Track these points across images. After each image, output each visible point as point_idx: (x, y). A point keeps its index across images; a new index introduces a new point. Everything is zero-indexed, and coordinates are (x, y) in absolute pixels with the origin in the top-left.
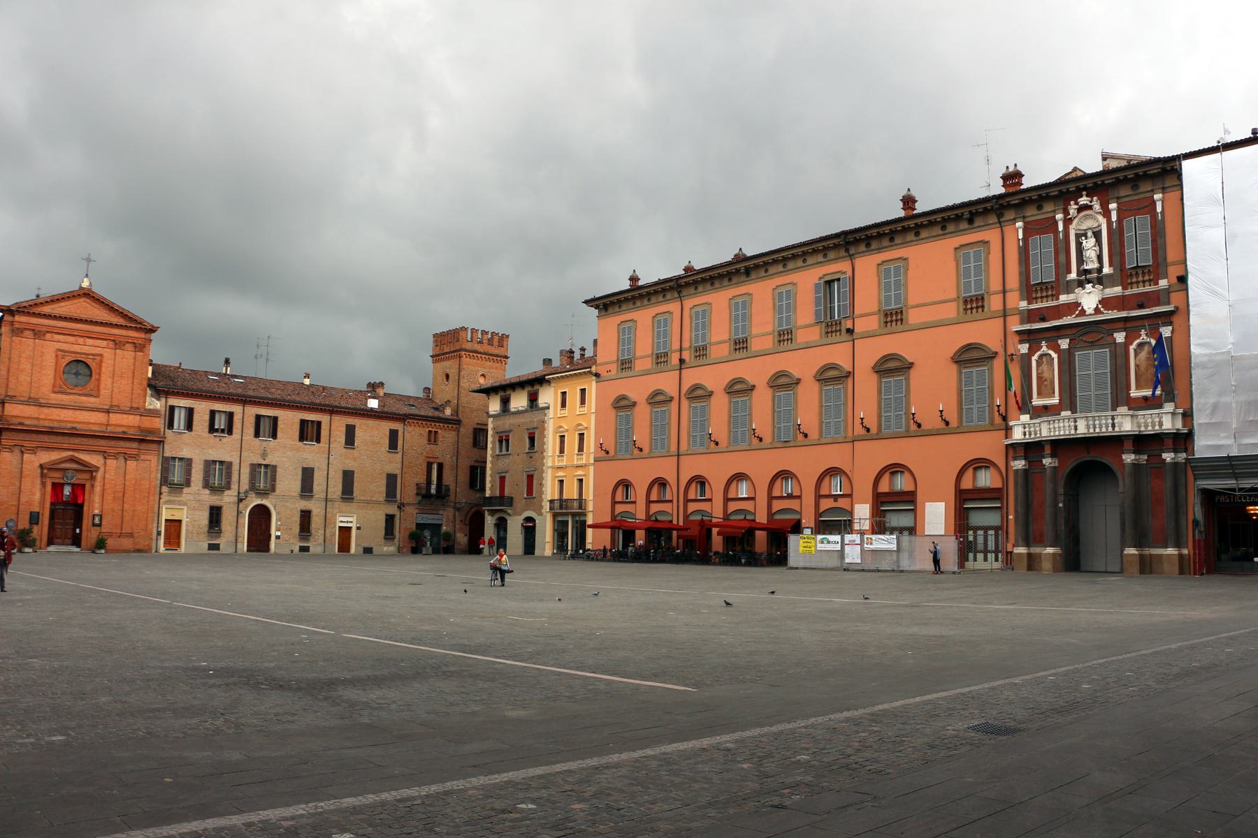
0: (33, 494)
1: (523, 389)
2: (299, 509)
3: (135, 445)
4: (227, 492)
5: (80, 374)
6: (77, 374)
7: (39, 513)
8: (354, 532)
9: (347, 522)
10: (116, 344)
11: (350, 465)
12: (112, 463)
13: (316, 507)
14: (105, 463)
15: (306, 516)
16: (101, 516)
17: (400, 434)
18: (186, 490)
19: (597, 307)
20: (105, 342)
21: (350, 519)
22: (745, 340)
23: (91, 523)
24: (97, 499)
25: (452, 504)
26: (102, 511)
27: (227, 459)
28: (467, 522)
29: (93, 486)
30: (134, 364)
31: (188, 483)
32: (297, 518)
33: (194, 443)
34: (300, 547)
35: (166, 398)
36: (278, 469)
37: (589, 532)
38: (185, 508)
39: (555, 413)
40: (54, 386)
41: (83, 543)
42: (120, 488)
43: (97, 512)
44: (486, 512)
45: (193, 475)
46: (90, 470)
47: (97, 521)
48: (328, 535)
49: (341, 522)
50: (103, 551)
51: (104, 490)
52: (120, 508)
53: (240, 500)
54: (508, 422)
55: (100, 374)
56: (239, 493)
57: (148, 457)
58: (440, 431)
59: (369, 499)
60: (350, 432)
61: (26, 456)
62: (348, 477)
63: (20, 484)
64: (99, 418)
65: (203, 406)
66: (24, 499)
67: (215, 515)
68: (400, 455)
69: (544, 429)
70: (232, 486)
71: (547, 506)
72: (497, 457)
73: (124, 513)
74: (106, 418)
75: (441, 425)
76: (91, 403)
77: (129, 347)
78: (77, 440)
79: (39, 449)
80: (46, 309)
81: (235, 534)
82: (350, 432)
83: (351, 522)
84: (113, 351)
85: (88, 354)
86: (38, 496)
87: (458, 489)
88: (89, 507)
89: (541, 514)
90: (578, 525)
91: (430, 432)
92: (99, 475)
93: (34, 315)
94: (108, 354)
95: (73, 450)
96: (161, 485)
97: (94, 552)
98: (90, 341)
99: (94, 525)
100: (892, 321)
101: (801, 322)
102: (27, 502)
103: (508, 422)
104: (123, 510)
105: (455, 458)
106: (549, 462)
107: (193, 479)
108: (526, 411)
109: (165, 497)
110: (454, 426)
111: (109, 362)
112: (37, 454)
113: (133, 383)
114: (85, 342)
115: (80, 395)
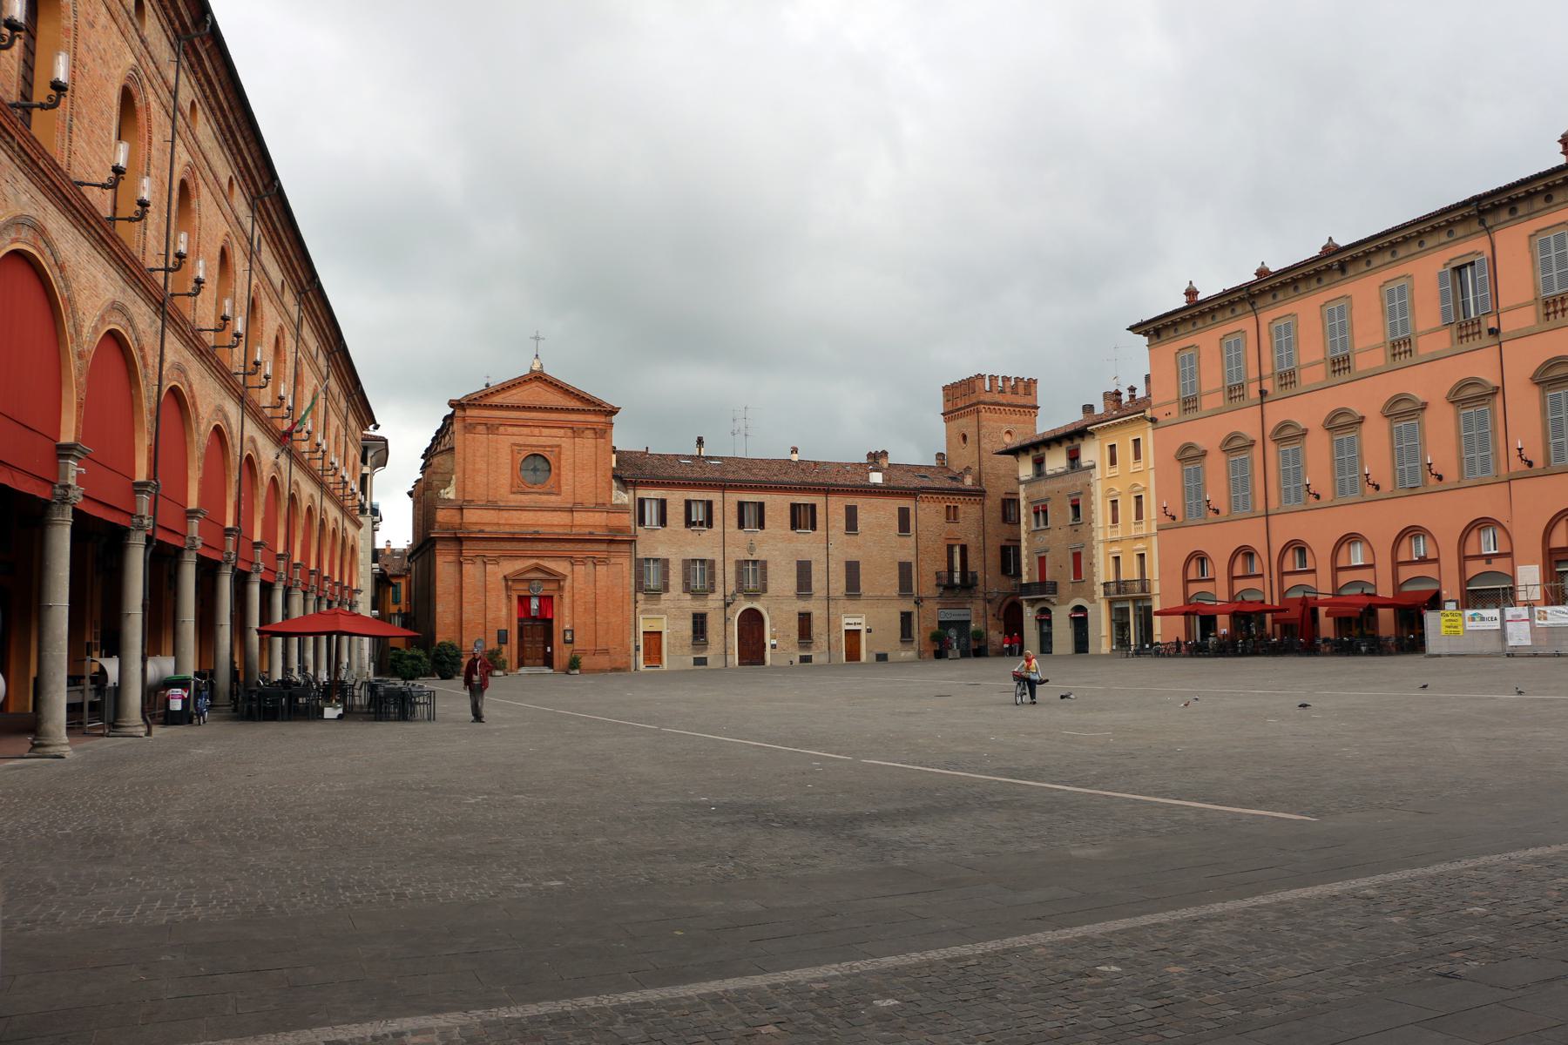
0: (500, 610)
1: (1061, 446)
2: (796, 611)
3: (604, 547)
4: (711, 596)
5: (538, 470)
6: (535, 470)
7: (506, 631)
8: (863, 635)
9: (855, 624)
10: (574, 432)
11: (854, 555)
12: (579, 569)
13: (816, 608)
15: (805, 619)
16: (573, 631)
17: (912, 512)
18: (664, 596)
19: (1146, 334)
20: (562, 431)
21: (858, 620)
22: (1346, 358)
23: (562, 640)
24: (567, 612)
25: (981, 595)
26: (573, 626)
27: (708, 557)
28: (1001, 617)
29: (561, 597)
30: (596, 454)
31: (666, 588)
32: (795, 623)
33: (670, 540)
34: (801, 657)
36: (768, 565)
37: (1157, 620)
38: (665, 617)
39: (1103, 471)
40: (512, 486)
41: (556, 663)
42: (591, 598)
43: (567, 626)
44: (1024, 602)
45: (671, 578)
46: (557, 579)
47: (568, 637)
48: (832, 641)
49: (848, 624)
50: (577, 672)
51: (573, 601)
52: (593, 621)
53: (727, 605)
54: (1044, 489)
55: (559, 468)
56: (725, 596)
57: (620, 560)
58: (960, 506)
59: (879, 594)
60: (851, 514)
61: (488, 567)
62: (852, 569)
66: (490, 616)
67: (699, 622)
68: (913, 538)
69: (1090, 494)
70: (717, 589)
71: (1100, 591)
72: (1033, 533)
74: (571, 518)
75: (962, 498)
77: (589, 434)
78: (540, 546)
79: (502, 558)
80: (497, 400)
81: (723, 646)
82: (851, 514)
83: (860, 624)
84: (572, 440)
85: (545, 447)
86: (504, 612)
87: (987, 576)
88: (559, 621)
89: (1093, 601)
90: (1142, 612)
91: (947, 507)
92: (567, 584)
93: (486, 407)
94: (566, 443)
96: (636, 592)
97: (567, 673)
98: (546, 431)
99: (566, 642)
100: (1555, 312)
101: (1421, 327)
102: (493, 619)
103: (1044, 489)
104: (596, 623)
105: (981, 538)
106: (1099, 535)
107: (671, 583)
108: (1066, 473)
109: (641, 606)
110: (978, 499)
111: (568, 453)
112: (501, 564)
114: (540, 432)
115: (540, 494)
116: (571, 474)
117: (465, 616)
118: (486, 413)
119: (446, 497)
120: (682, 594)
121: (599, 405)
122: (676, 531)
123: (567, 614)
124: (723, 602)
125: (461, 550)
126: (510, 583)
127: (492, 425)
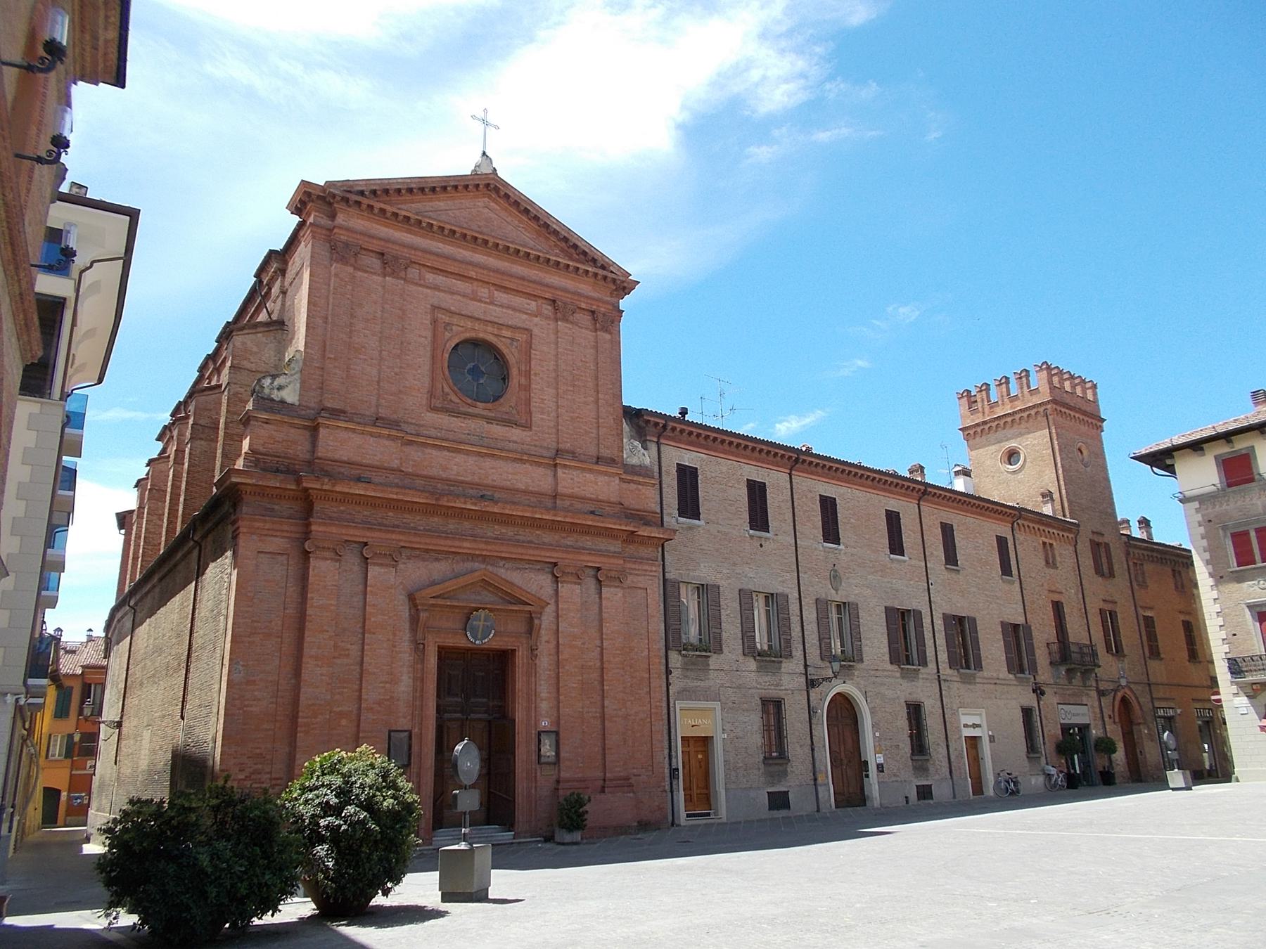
1: (1204, 455)
3: (615, 546)
6: (475, 372)
8: (986, 741)
10: (556, 309)
14: (557, 591)
16: (557, 733)
21: (977, 720)
24: (544, 690)
26: (558, 724)
27: (777, 588)
29: (533, 651)
33: (717, 550)
35: (658, 444)
38: (717, 705)
40: (431, 394)
41: (520, 815)
43: (545, 724)
47: (547, 749)
49: (966, 726)
50: (577, 836)
53: (811, 684)
55: (528, 374)
56: (806, 666)
61: (373, 571)
63: (363, 650)
64: (534, 478)
65: (724, 469)
66: (372, 694)
74: (550, 479)
76: (515, 442)
77: (585, 319)
79: (408, 552)
80: (409, 208)
81: (811, 767)
83: (979, 726)
86: (405, 685)
91: (1044, 543)
92: (547, 620)
94: (542, 327)
95: (484, 559)
96: (667, 649)
97: (549, 839)
98: (501, 297)
102: (379, 703)
107: (724, 635)
109: (677, 683)
112: (401, 566)
113: (597, 401)
115: (490, 420)
116: (552, 391)
117: (306, 693)
118: (383, 231)
119: (276, 395)
120: (741, 658)
121: (603, 267)
122: (726, 534)
123: (544, 695)
124: (803, 679)
125: (308, 525)
126: (423, 615)
127: (396, 258)
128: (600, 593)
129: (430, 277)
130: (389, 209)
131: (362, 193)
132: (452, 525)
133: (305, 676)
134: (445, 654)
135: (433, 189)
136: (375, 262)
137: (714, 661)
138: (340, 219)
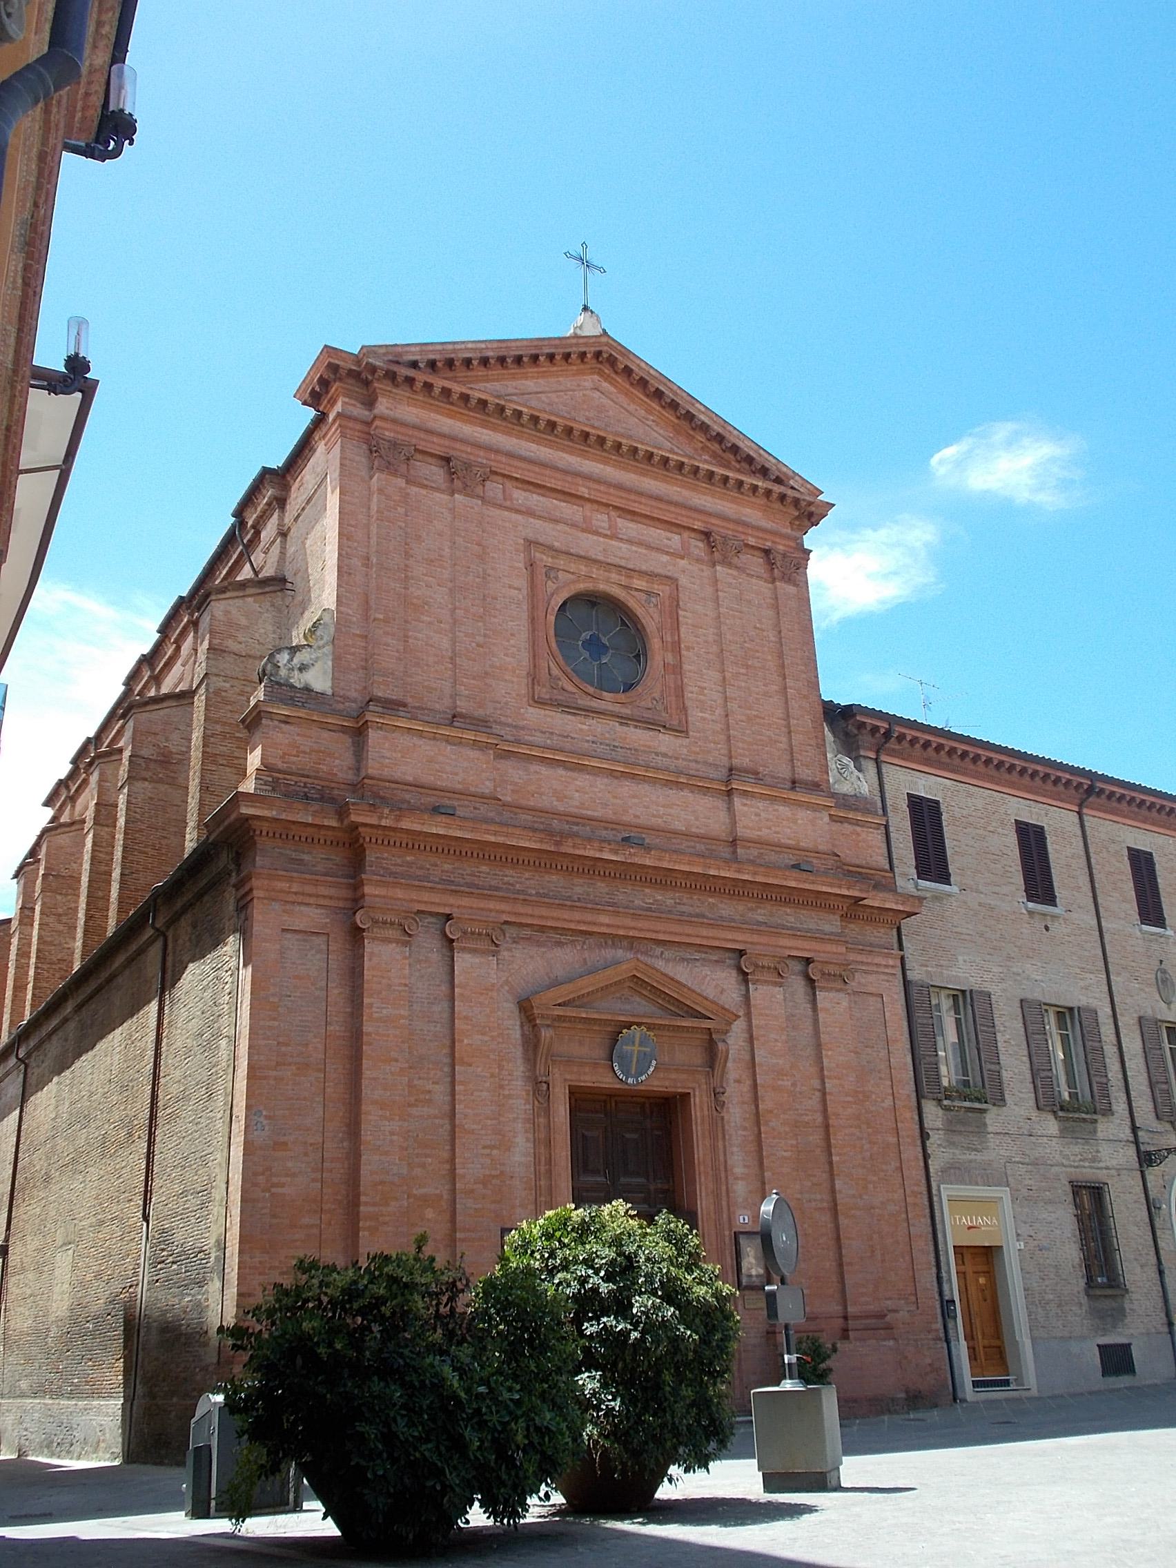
0: (505, 1145)
6: (596, 647)
10: (711, 546)
14: (747, 997)
27: (1075, 997)
29: (717, 1095)
33: (982, 935)
38: (1004, 1193)
40: (534, 679)
55: (676, 647)
56: (1134, 1129)
61: (463, 961)
63: (453, 1094)
65: (980, 804)
66: (471, 1168)
73: (843, 1221)
74: (723, 816)
76: (665, 755)
77: (756, 563)
79: (511, 931)
80: (486, 387)
81: (1160, 1304)
85: (631, 572)
88: (717, 1196)
92: (735, 1042)
95: (631, 942)
96: (919, 1096)
102: (485, 1182)
104: (834, 1210)
107: (1005, 1075)
115: (624, 720)
116: (715, 675)
117: (370, 1165)
118: (445, 423)
119: (298, 680)
120: (1034, 1114)
121: (778, 481)
122: (992, 909)
123: (739, 1170)
124: (1131, 1152)
125: (357, 886)
126: (546, 1034)
127: (468, 466)
128: (814, 1001)
129: (521, 496)
130: (457, 388)
131: (414, 365)
132: (580, 887)
133: (367, 1135)
134: (580, 1100)
135: (518, 360)
136: (436, 473)
137: (994, 1119)
138: (383, 406)
